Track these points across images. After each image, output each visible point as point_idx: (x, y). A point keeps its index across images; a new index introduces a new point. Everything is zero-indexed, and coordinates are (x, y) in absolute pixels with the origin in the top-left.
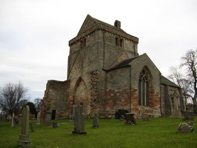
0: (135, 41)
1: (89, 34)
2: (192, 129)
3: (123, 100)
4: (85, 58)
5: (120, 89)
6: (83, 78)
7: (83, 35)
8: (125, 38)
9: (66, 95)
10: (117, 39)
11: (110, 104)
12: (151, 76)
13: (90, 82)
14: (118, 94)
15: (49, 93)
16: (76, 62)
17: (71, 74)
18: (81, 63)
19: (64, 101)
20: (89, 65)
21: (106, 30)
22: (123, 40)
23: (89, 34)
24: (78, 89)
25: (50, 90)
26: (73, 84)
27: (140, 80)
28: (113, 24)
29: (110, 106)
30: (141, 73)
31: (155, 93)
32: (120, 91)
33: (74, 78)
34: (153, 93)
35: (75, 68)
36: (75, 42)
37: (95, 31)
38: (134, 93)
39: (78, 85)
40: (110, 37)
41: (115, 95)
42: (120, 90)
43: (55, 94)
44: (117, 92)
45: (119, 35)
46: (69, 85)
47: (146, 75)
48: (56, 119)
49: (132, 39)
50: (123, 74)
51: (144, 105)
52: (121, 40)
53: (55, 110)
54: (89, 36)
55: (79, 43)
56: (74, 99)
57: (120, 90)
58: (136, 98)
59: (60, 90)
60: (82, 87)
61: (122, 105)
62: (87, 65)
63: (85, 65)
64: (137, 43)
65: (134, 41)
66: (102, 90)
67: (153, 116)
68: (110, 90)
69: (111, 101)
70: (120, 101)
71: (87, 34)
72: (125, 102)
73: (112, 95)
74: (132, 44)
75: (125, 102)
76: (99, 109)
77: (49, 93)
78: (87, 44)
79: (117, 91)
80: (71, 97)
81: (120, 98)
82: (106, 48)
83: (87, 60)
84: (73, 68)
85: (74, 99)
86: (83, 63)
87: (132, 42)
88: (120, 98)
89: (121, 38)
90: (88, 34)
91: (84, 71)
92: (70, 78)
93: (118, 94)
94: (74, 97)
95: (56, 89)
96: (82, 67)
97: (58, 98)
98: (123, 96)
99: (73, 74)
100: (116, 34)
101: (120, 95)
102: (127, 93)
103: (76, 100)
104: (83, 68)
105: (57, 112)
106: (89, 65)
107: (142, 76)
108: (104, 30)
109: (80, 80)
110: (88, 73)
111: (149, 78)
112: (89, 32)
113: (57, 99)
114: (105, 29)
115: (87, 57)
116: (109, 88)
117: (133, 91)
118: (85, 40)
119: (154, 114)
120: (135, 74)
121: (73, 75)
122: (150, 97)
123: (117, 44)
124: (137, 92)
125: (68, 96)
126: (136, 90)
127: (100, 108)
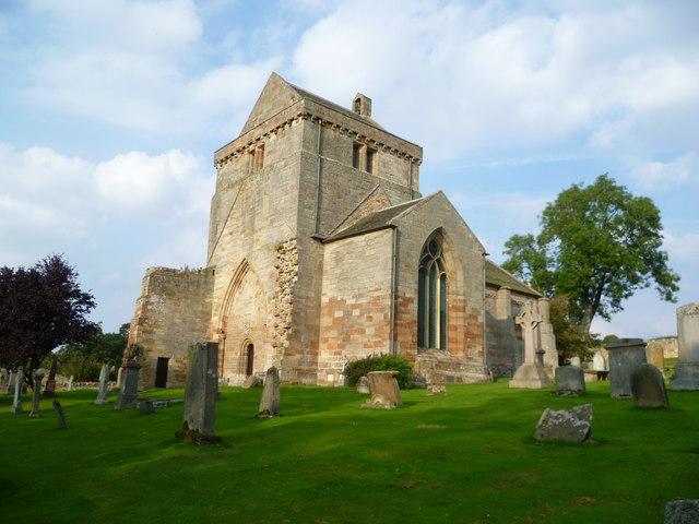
0: (410, 155)
1: (275, 131)
2: (586, 431)
3: (370, 331)
4: (260, 202)
5: (361, 296)
6: (253, 263)
7: (258, 133)
9: (202, 312)
10: (356, 147)
11: (330, 341)
13: (271, 276)
14: (356, 313)
15: (149, 307)
16: (236, 216)
17: (218, 251)
18: (247, 219)
19: (194, 331)
20: (272, 222)
21: (326, 118)
23: (275, 131)
24: (237, 295)
25: (154, 299)
26: (222, 281)
28: (349, 106)
29: (330, 347)
30: (425, 251)
32: (361, 305)
33: (227, 263)
35: (231, 234)
36: (232, 155)
37: (292, 120)
39: (237, 282)
41: (348, 314)
42: (363, 301)
43: (166, 311)
44: (354, 307)
45: (364, 137)
46: (213, 283)
48: (168, 385)
49: (403, 149)
50: (373, 252)
51: (432, 345)
52: (370, 153)
53: (167, 360)
54: (273, 136)
55: (246, 157)
56: (225, 324)
57: (363, 301)
58: (410, 324)
60: (248, 289)
61: (366, 346)
62: (267, 223)
63: (258, 224)
64: (416, 162)
67: (460, 379)
68: (332, 300)
69: (333, 333)
70: (362, 332)
71: (268, 130)
72: (376, 335)
73: (338, 314)
74: (403, 164)
75: (376, 335)
76: (298, 356)
78: (267, 161)
79: (353, 302)
80: (215, 321)
81: (362, 324)
83: (265, 210)
84: (226, 231)
85: (225, 324)
86: (253, 217)
87: (402, 160)
88: (362, 324)
89: (373, 146)
90: (272, 131)
91: (258, 240)
92: (214, 262)
93: (356, 313)
94: (224, 320)
95: (170, 294)
96: (251, 229)
98: (370, 318)
99: (223, 250)
101: (362, 315)
102: (382, 310)
103: (229, 330)
104: (253, 231)
106: (272, 222)
107: (428, 258)
108: (318, 119)
109: (244, 267)
110: (267, 247)
112: (273, 127)
113: (174, 324)
114: (319, 115)
115: (266, 199)
116: (330, 294)
118: (262, 147)
119: (462, 373)
121: (223, 253)
122: (451, 323)
123: (355, 163)
124: (414, 307)
125: (207, 315)
126: (410, 300)
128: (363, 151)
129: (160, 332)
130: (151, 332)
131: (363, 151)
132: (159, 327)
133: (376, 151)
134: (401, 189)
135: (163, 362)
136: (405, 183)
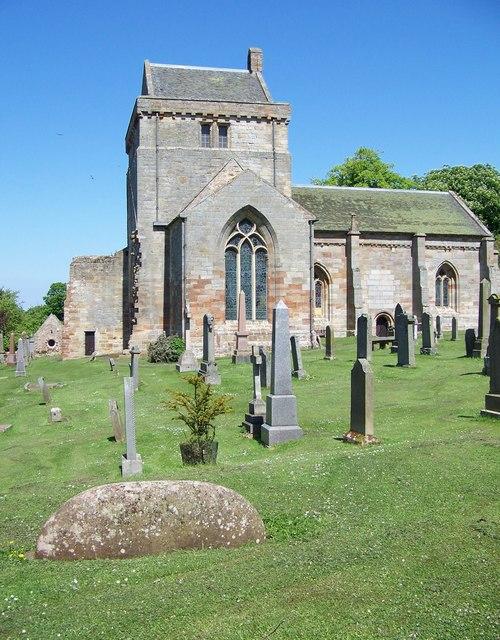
8: (234, 117)
10: (206, 128)
12: (272, 232)
21: (163, 110)
22: (229, 124)
27: (232, 251)
31: (287, 281)
34: (278, 281)
38: (198, 290)
40: (179, 126)
45: (210, 116)
47: (257, 230)
49: (262, 114)
52: (224, 129)
53: (93, 333)
59: (102, 279)
65: (273, 118)
66: (154, 280)
77: (73, 291)
82: (164, 162)
87: (264, 124)
97: (98, 300)
100: (199, 115)
105: (97, 335)
108: (154, 113)
111: (267, 239)
117: (195, 287)
120: (204, 240)
126: (208, 282)
127: (151, 328)
128: (215, 129)
129: (84, 311)
130: (75, 312)
131: (215, 129)
132: (84, 306)
133: (229, 124)
134: (262, 156)
135: (90, 335)
136: (269, 147)
